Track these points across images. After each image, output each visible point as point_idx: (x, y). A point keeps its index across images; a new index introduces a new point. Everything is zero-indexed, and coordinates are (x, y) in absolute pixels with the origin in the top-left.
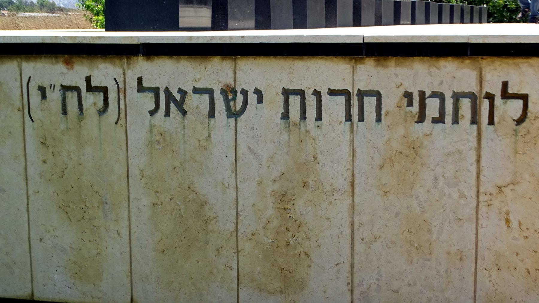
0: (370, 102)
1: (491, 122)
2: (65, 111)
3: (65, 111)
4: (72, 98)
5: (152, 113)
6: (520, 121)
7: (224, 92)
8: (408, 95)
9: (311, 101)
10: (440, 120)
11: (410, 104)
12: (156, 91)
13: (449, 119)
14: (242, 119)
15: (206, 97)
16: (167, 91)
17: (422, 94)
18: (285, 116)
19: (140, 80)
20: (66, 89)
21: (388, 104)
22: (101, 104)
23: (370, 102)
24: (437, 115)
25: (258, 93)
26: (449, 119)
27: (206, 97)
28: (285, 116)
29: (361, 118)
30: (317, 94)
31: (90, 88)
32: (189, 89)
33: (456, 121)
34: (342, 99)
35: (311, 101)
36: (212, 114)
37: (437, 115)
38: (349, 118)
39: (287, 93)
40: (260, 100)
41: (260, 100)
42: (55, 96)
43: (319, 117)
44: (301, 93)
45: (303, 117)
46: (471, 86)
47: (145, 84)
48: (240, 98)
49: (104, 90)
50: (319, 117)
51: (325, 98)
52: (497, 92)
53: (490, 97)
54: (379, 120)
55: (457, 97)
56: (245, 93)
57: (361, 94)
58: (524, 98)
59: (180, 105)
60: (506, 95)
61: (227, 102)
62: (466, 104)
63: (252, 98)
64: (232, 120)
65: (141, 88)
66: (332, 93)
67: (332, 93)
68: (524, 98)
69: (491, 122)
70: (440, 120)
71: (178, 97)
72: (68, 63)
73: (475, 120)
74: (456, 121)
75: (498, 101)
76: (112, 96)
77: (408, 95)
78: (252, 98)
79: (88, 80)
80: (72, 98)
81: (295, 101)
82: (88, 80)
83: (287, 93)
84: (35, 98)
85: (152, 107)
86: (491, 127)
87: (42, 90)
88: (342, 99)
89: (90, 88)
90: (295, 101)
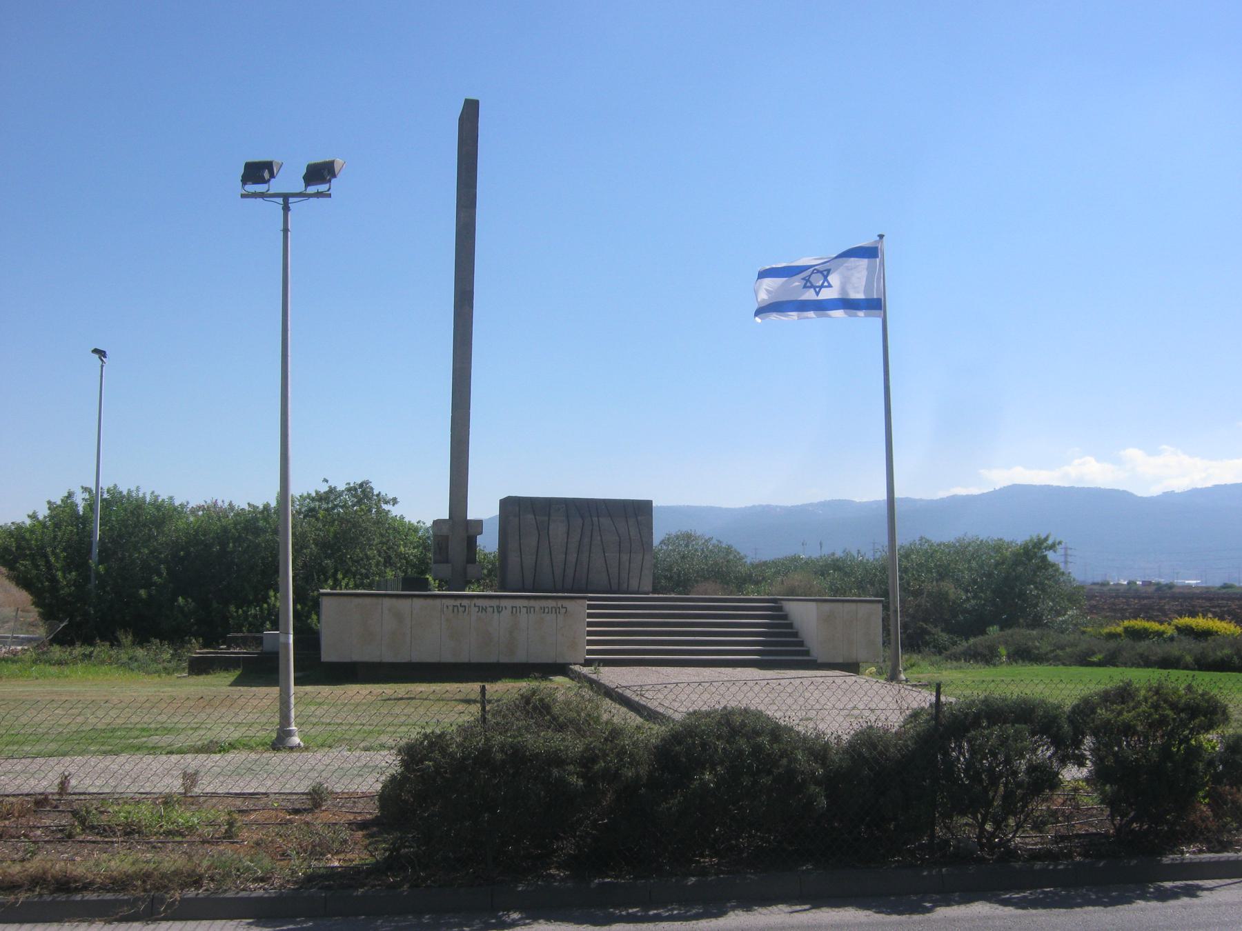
0: (532, 609)
2: (453, 612)
3: (453, 612)
4: (456, 609)
7: (497, 607)
10: (548, 613)
12: (479, 607)
15: (492, 609)
16: (482, 607)
18: (512, 612)
20: (454, 606)
21: (537, 609)
23: (532, 609)
28: (512, 612)
31: (461, 606)
32: (488, 606)
34: (525, 609)
36: (494, 612)
39: (512, 607)
42: (451, 608)
49: (465, 607)
57: (530, 607)
62: (554, 610)
65: (475, 606)
66: (524, 607)
67: (524, 607)
68: (566, 608)
70: (548, 613)
72: (456, 600)
73: (556, 613)
77: (541, 608)
78: (504, 609)
79: (461, 604)
80: (456, 609)
81: (514, 609)
82: (461, 604)
84: (445, 609)
88: (525, 609)
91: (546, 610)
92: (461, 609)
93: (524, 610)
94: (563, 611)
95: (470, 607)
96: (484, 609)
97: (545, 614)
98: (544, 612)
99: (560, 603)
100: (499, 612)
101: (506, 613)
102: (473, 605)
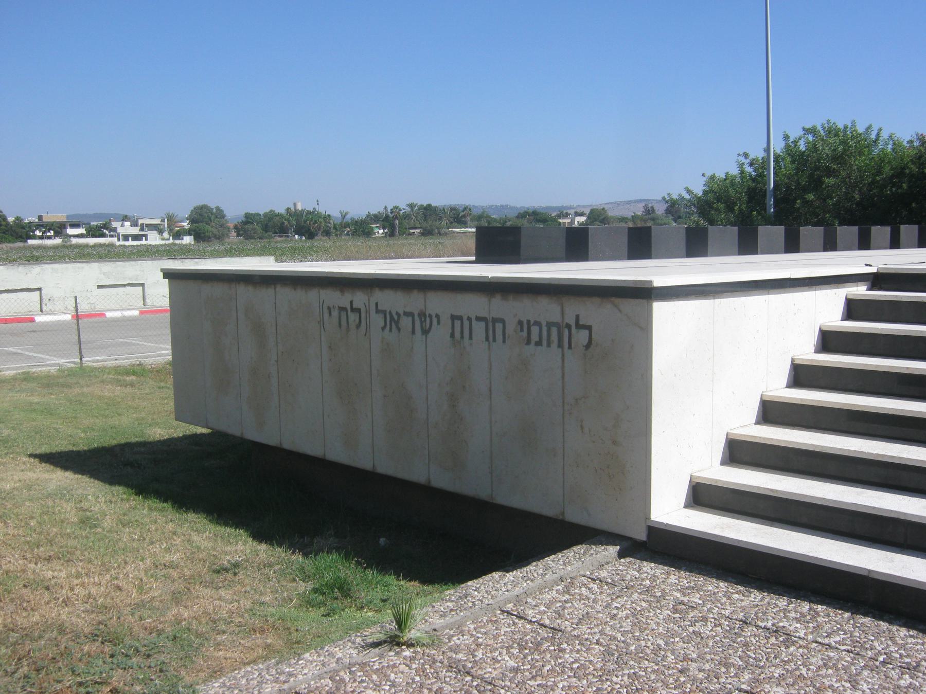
1: (570, 347)
5: (383, 328)
6: (588, 346)
7: (419, 315)
8: (520, 323)
9: (466, 323)
10: (539, 343)
11: (522, 330)
12: (384, 312)
13: (545, 342)
14: (431, 334)
15: (410, 318)
16: (390, 313)
17: (528, 322)
18: (452, 335)
19: (377, 304)
22: (357, 320)
23: (499, 326)
24: (538, 340)
25: (437, 316)
26: (545, 342)
27: (410, 318)
29: (494, 340)
30: (469, 319)
31: (353, 310)
32: (401, 312)
33: (549, 345)
34: (483, 324)
35: (466, 323)
36: (413, 332)
37: (538, 340)
38: (487, 339)
40: (439, 323)
41: (439, 323)
42: (335, 313)
43: (471, 338)
44: (460, 318)
45: (462, 337)
46: (556, 318)
47: (380, 308)
48: (428, 320)
49: (358, 311)
50: (471, 338)
51: (474, 322)
52: (572, 323)
53: (568, 326)
54: (504, 341)
55: (550, 325)
56: (430, 316)
57: (495, 320)
58: (589, 328)
59: (397, 323)
60: (579, 326)
61: (421, 322)
62: (554, 331)
63: (435, 320)
64: (424, 337)
65: (378, 311)
66: (479, 319)
67: (479, 319)
68: (589, 328)
69: (570, 347)
71: (396, 317)
72: (342, 292)
73: (560, 345)
74: (549, 345)
75: (574, 330)
76: (363, 315)
77: (520, 323)
78: (435, 320)
81: (458, 323)
83: (453, 318)
84: (326, 315)
85: (382, 324)
86: (570, 351)
87: (329, 308)
88: (483, 324)
89: (353, 310)
90: (458, 323)
91: (535, 330)
92: (353, 317)
93: (479, 328)
94: (581, 337)
95: (368, 312)
96: (392, 321)
97: (532, 346)
98: (528, 342)
99: (573, 308)
100: (425, 332)
101: (440, 333)
102: (373, 307)
